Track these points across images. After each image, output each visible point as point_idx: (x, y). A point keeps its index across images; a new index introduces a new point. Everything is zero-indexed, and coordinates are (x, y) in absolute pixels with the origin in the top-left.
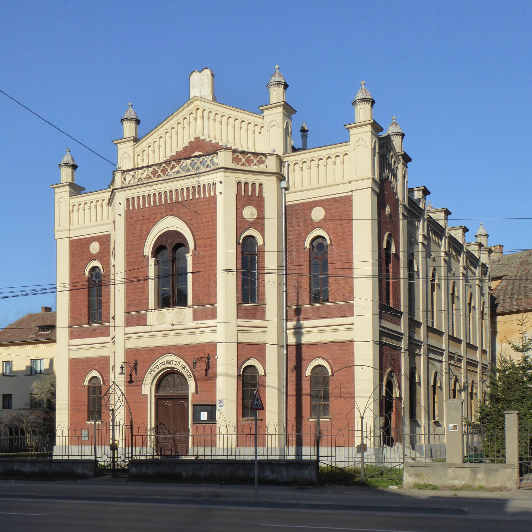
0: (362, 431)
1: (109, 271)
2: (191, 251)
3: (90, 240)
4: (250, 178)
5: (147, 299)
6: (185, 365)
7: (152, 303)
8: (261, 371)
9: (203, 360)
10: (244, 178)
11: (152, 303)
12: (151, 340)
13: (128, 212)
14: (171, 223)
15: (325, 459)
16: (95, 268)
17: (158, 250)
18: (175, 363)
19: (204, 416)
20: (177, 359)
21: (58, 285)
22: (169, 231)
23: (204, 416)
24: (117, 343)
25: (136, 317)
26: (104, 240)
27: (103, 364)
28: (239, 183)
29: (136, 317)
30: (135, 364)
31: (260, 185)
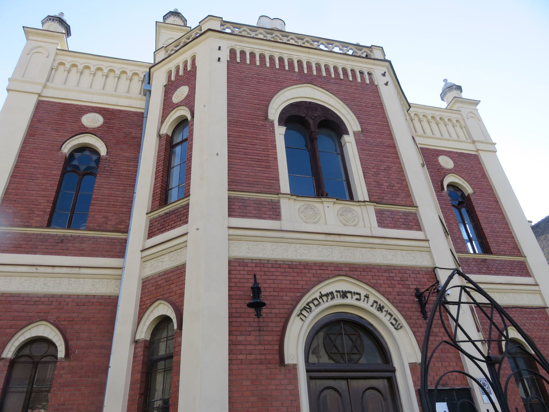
2: (351, 132)
5: (277, 179)
6: (383, 301)
18: (358, 297)
22: (310, 103)
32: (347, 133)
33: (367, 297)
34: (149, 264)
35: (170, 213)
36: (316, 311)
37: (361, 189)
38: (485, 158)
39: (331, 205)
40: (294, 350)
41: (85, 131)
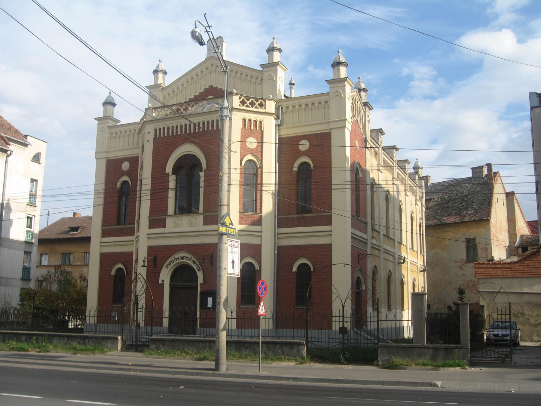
0: (343, 317)
1: (136, 185)
2: (203, 170)
3: (121, 161)
4: (253, 117)
6: (196, 260)
7: (171, 209)
8: (257, 268)
10: (248, 116)
11: (171, 209)
13: (155, 139)
14: (187, 149)
15: (313, 340)
17: (176, 170)
19: (210, 300)
20: (189, 256)
21: (93, 196)
22: (187, 155)
23: (210, 300)
24: (142, 240)
25: (158, 220)
26: (134, 161)
27: (127, 258)
28: (244, 120)
29: (158, 220)
30: (157, 257)
31: (261, 122)
33: (191, 259)
36: (172, 265)
39: (185, 217)
41: (123, 173)
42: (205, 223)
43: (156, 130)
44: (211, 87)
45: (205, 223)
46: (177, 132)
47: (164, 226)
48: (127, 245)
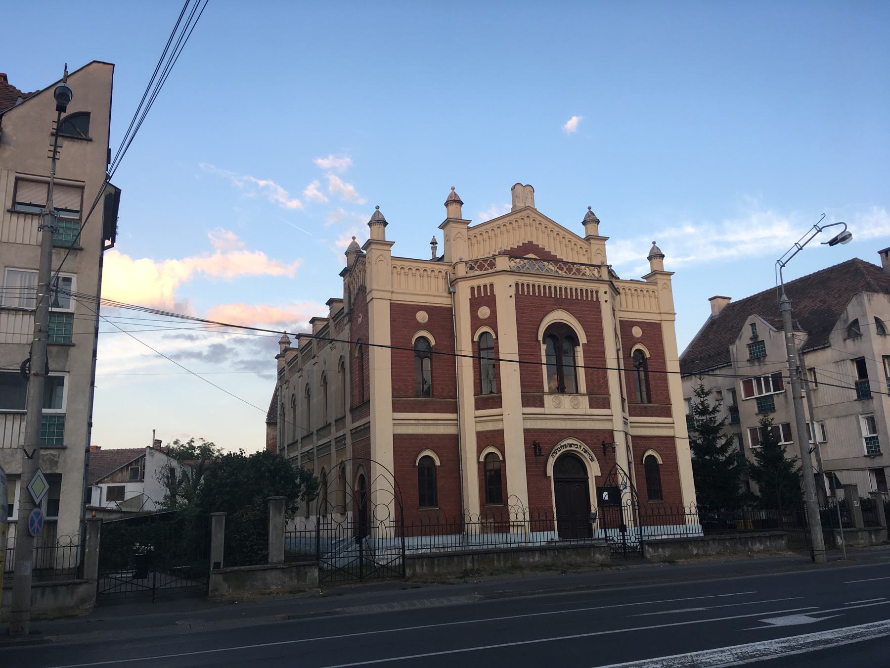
6: (588, 448)
9: (604, 445)
12: (549, 422)
14: (559, 316)
16: (638, 350)
32: (579, 345)
34: (479, 424)
35: (488, 398)
37: (583, 388)
38: (665, 327)
40: (550, 472)
42: (591, 406)
43: (517, 284)
44: (530, 243)
45: (591, 406)
46: (545, 293)
47: (542, 405)
48: (437, 424)
